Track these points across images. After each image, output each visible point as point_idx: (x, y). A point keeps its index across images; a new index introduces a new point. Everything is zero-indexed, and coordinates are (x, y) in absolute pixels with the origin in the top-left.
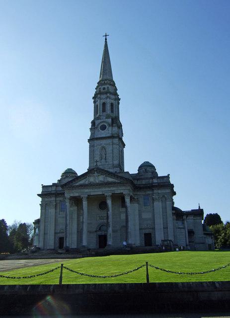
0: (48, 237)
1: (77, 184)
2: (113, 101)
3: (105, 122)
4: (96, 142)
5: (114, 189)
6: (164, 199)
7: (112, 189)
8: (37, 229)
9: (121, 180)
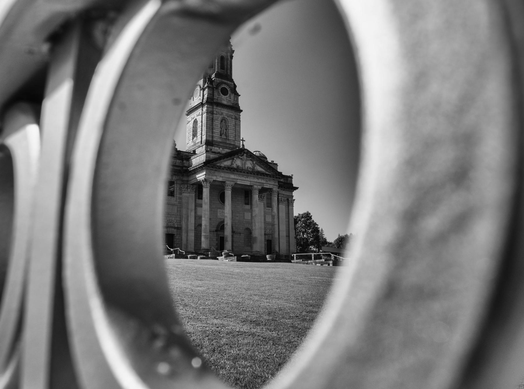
4: (217, 109)
5: (263, 181)
6: (286, 202)
7: (260, 181)
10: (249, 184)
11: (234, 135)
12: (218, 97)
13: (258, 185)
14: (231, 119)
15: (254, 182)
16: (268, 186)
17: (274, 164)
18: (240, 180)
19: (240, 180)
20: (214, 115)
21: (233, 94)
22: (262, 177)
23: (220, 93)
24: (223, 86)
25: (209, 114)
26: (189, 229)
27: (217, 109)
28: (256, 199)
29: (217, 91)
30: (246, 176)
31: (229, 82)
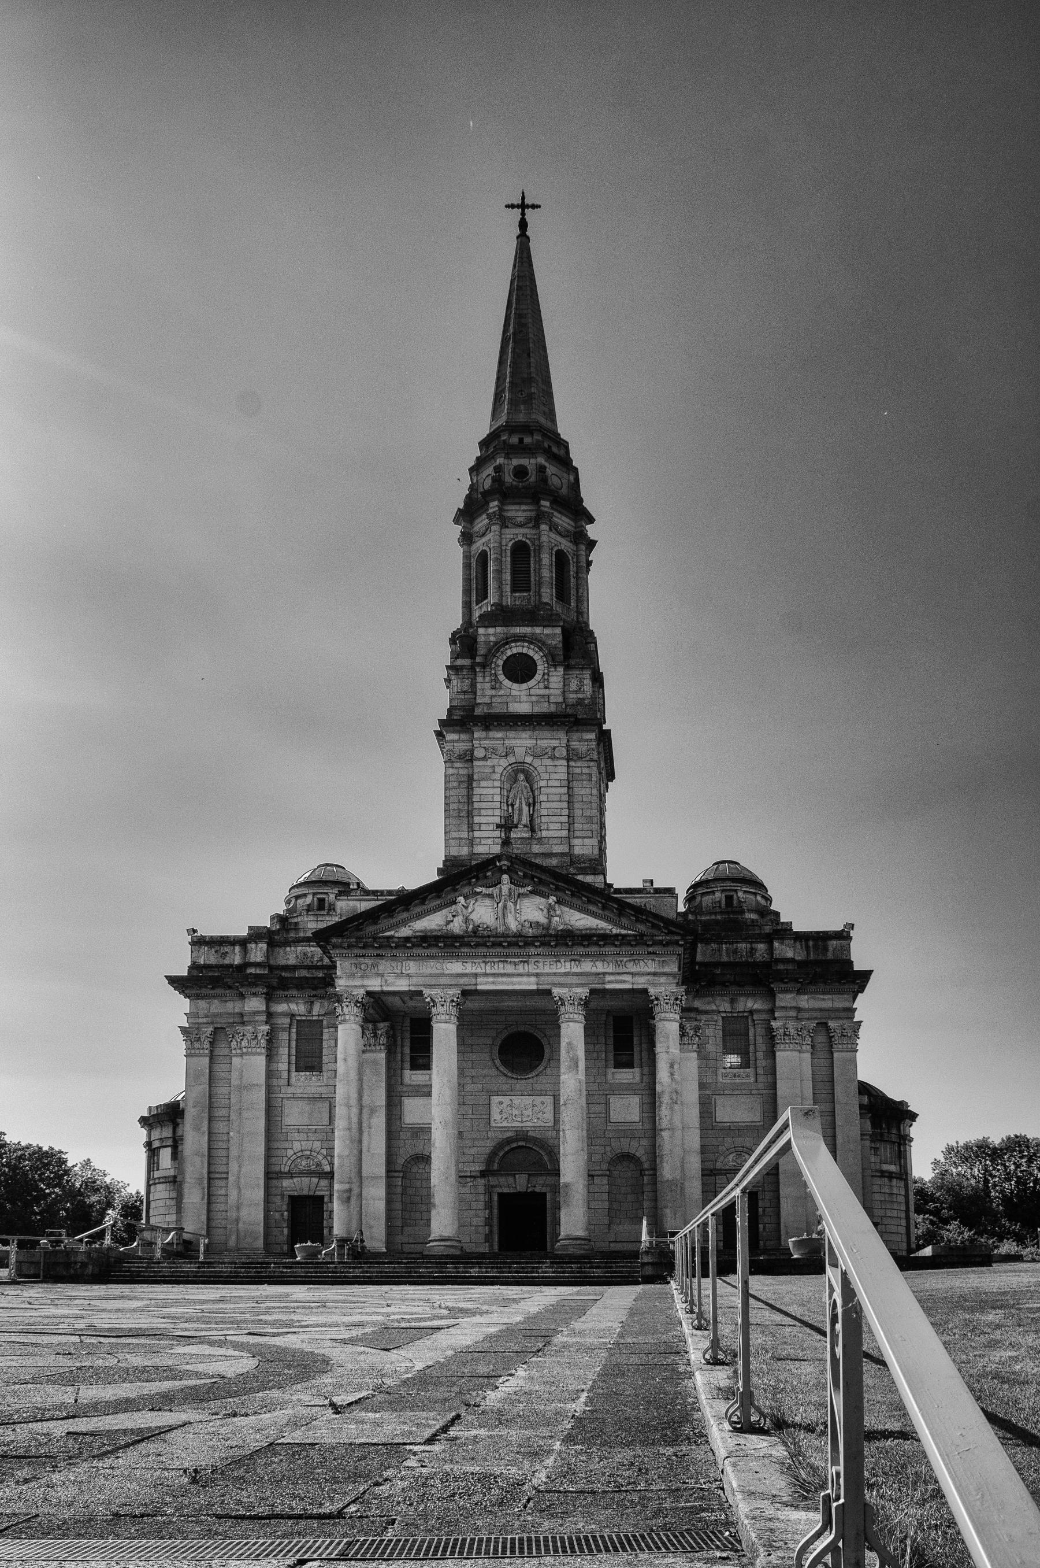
0: (233, 1193)
1: (405, 932)
2: (566, 545)
3: (532, 640)
4: (483, 741)
5: (600, 967)
6: (821, 1039)
7: (587, 966)
8: (166, 1155)
9: (642, 928)
10: (534, 987)
11: (565, 819)
12: (492, 696)
13: (570, 986)
14: (549, 762)
15: (555, 974)
16: (624, 982)
17: (658, 891)
18: (486, 975)
19: (486, 975)
20: (476, 763)
21: (561, 669)
22: (593, 949)
23: (502, 677)
24: (515, 651)
25: (457, 765)
26: (365, 1172)
27: (486, 738)
28: (567, 1040)
29: (487, 674)
30: (516, 956)
31: (538, 630)
